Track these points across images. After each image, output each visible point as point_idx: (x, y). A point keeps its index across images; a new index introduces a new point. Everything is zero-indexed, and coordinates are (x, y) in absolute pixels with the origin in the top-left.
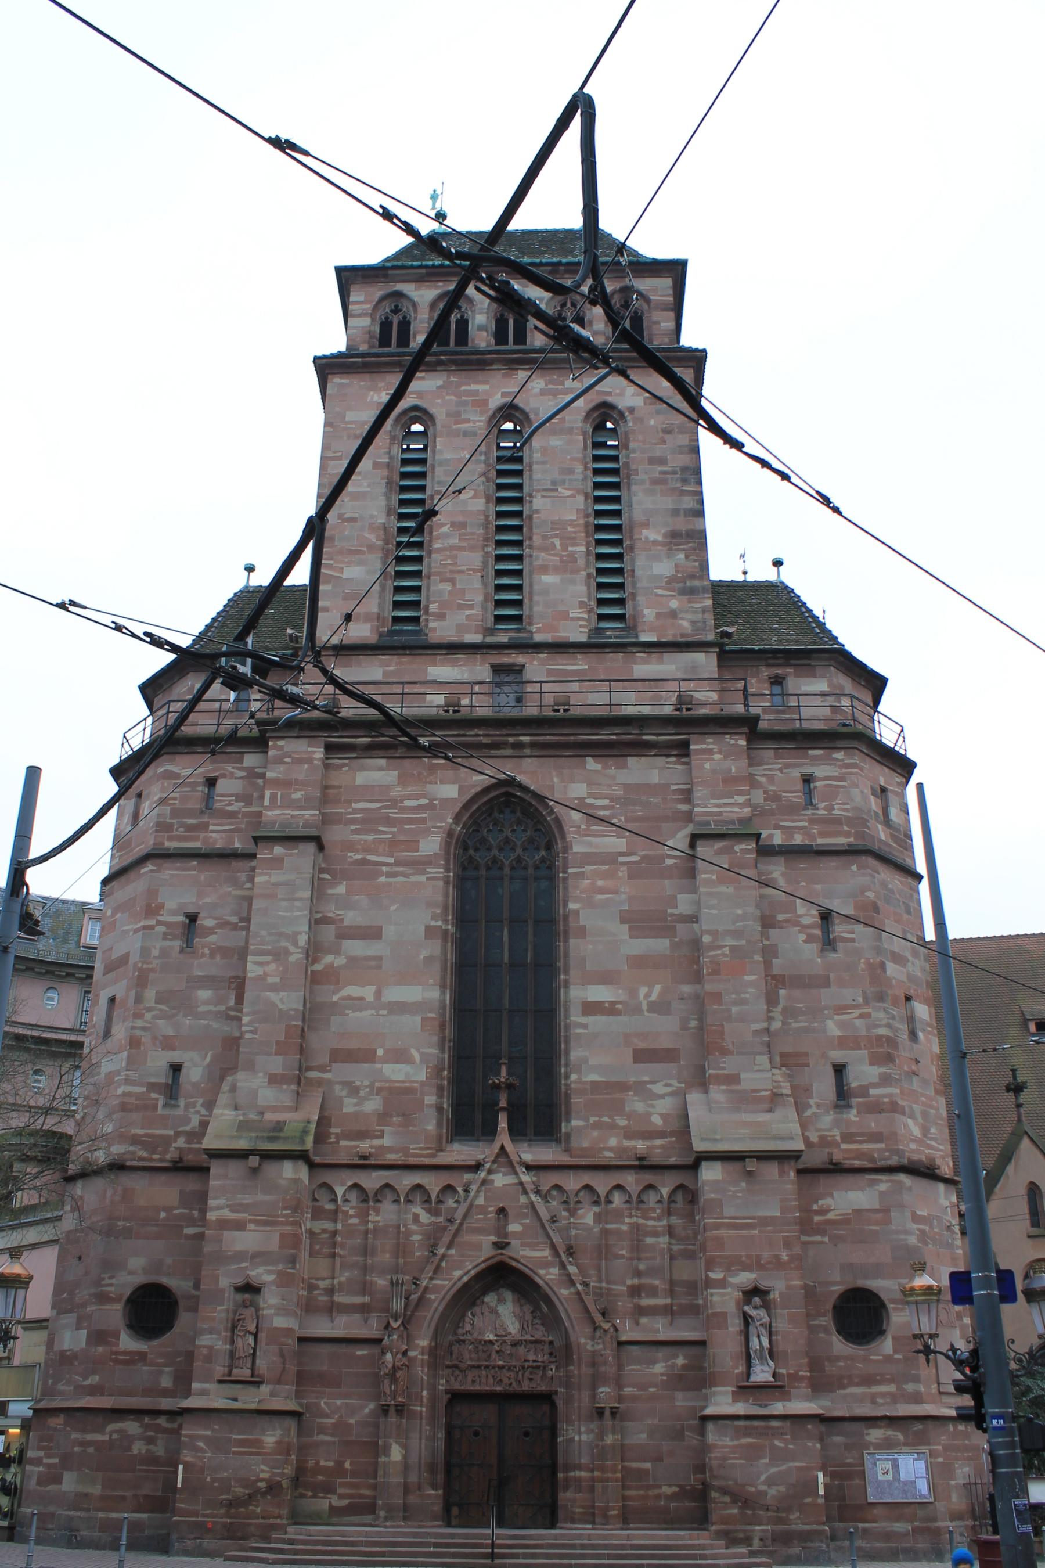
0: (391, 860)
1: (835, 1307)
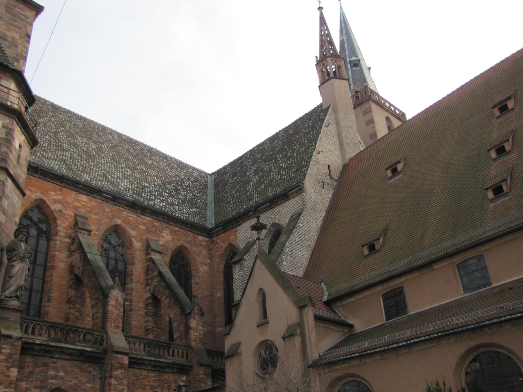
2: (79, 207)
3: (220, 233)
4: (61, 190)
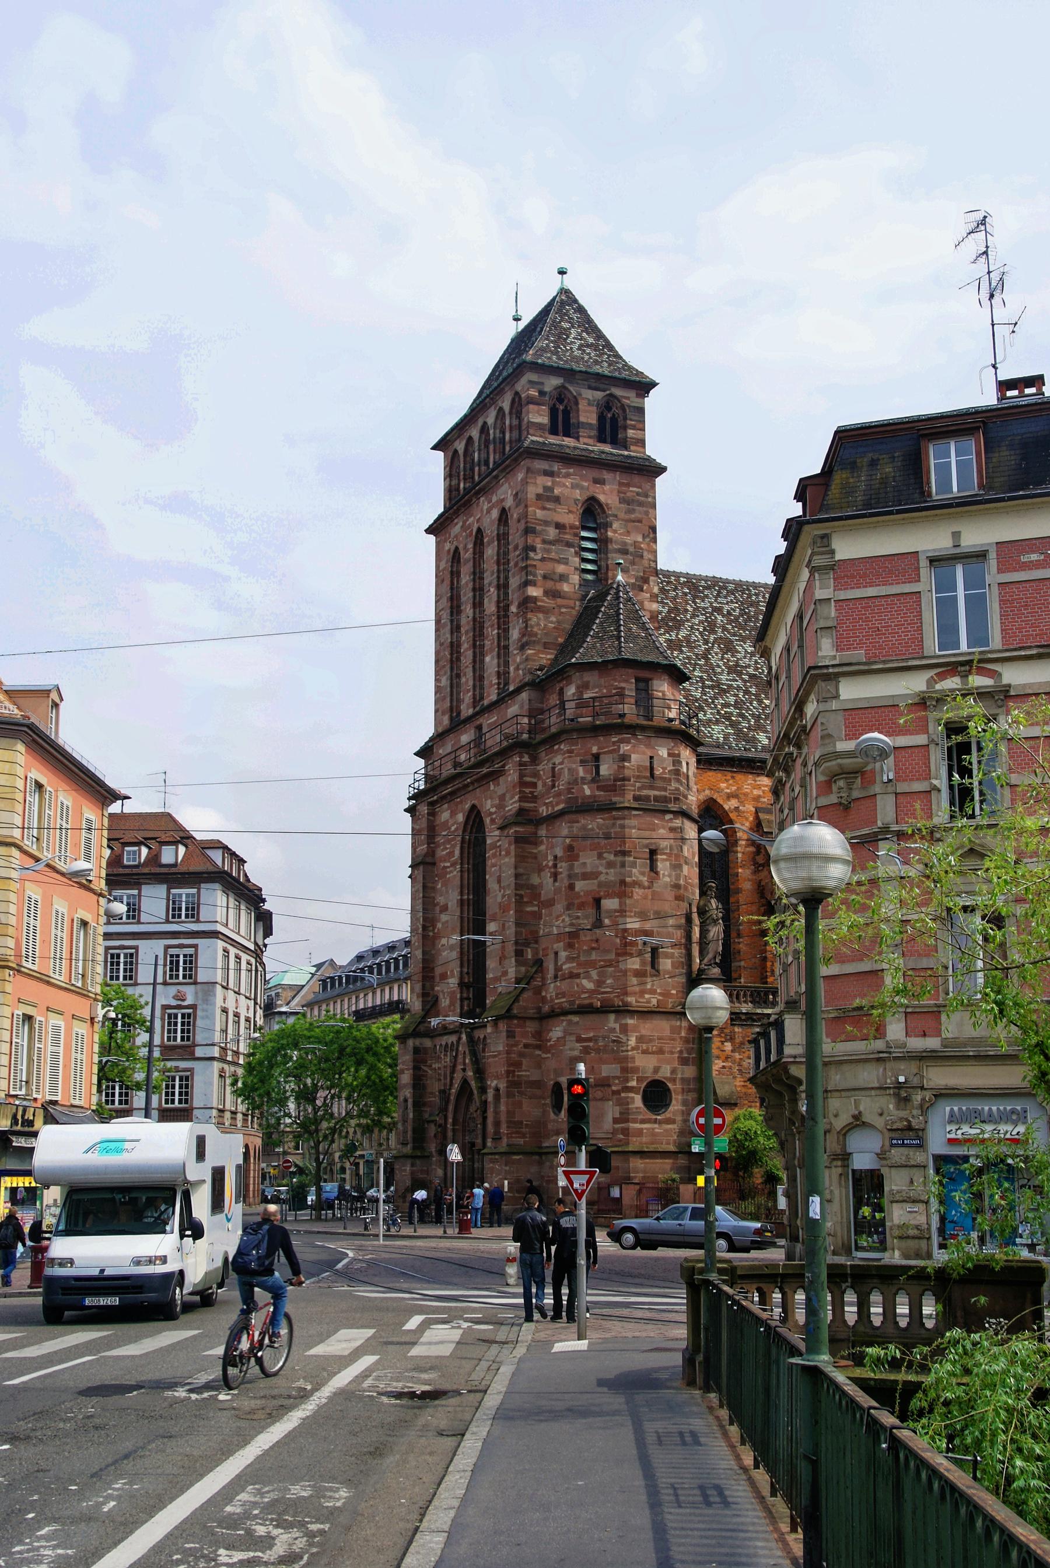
0: (448, 864)
1: (553, 1091)
2: (759, 796)
4: (733, 777)
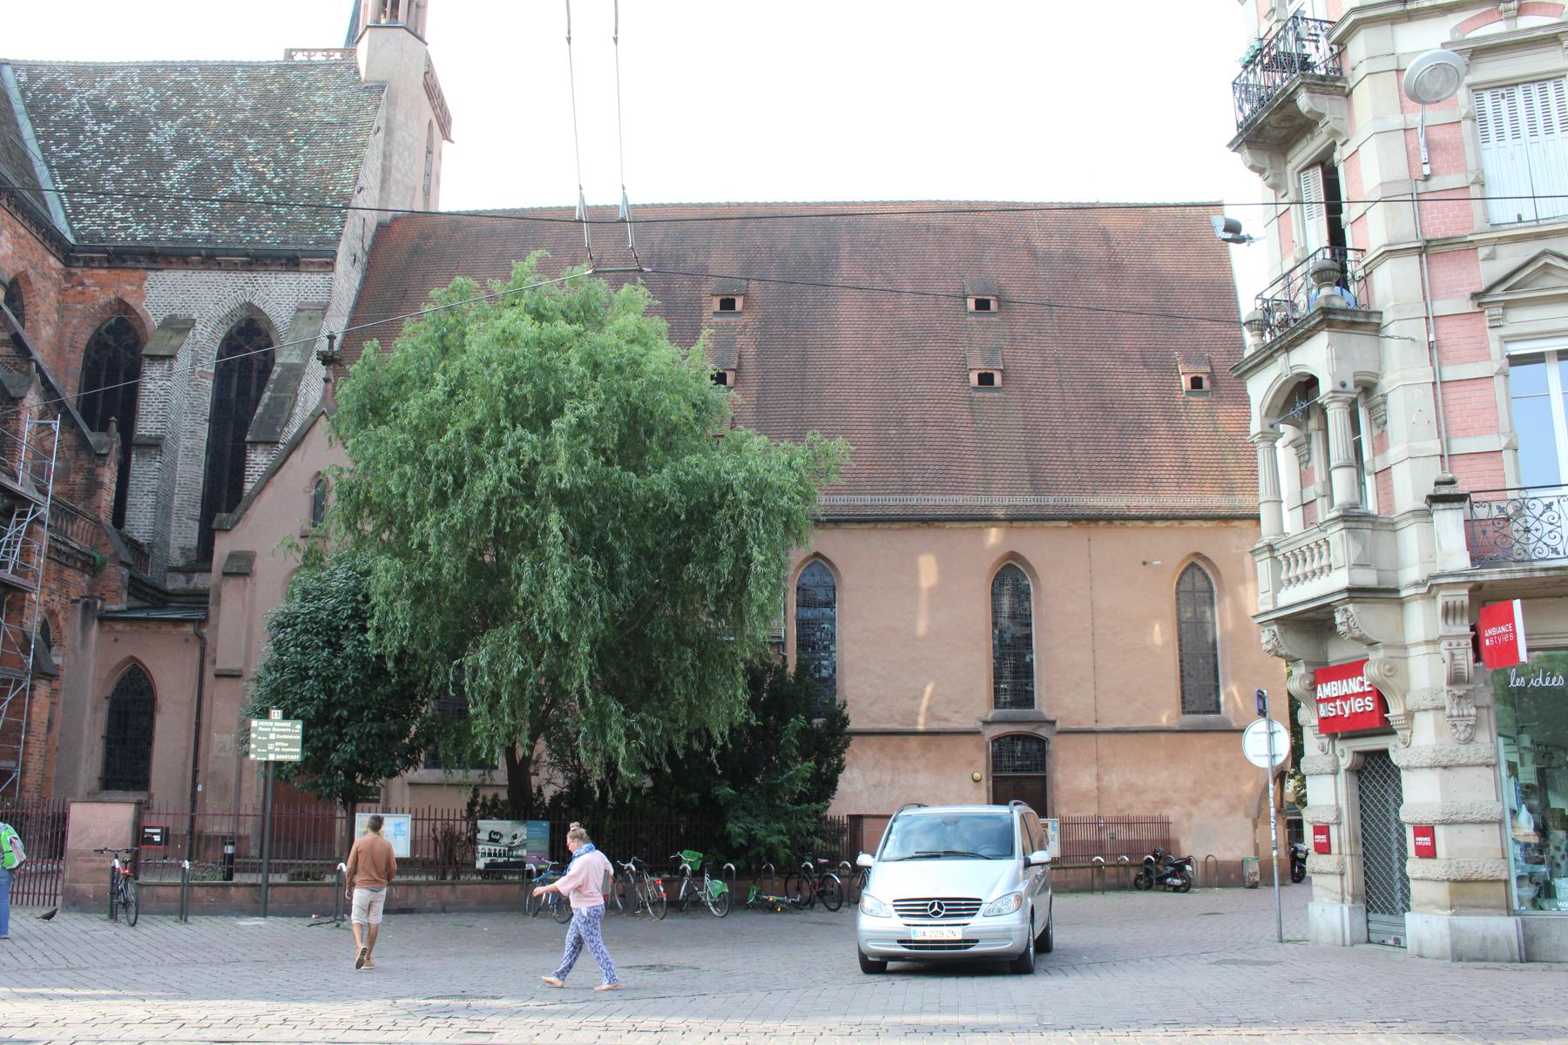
3: (96, 264)
